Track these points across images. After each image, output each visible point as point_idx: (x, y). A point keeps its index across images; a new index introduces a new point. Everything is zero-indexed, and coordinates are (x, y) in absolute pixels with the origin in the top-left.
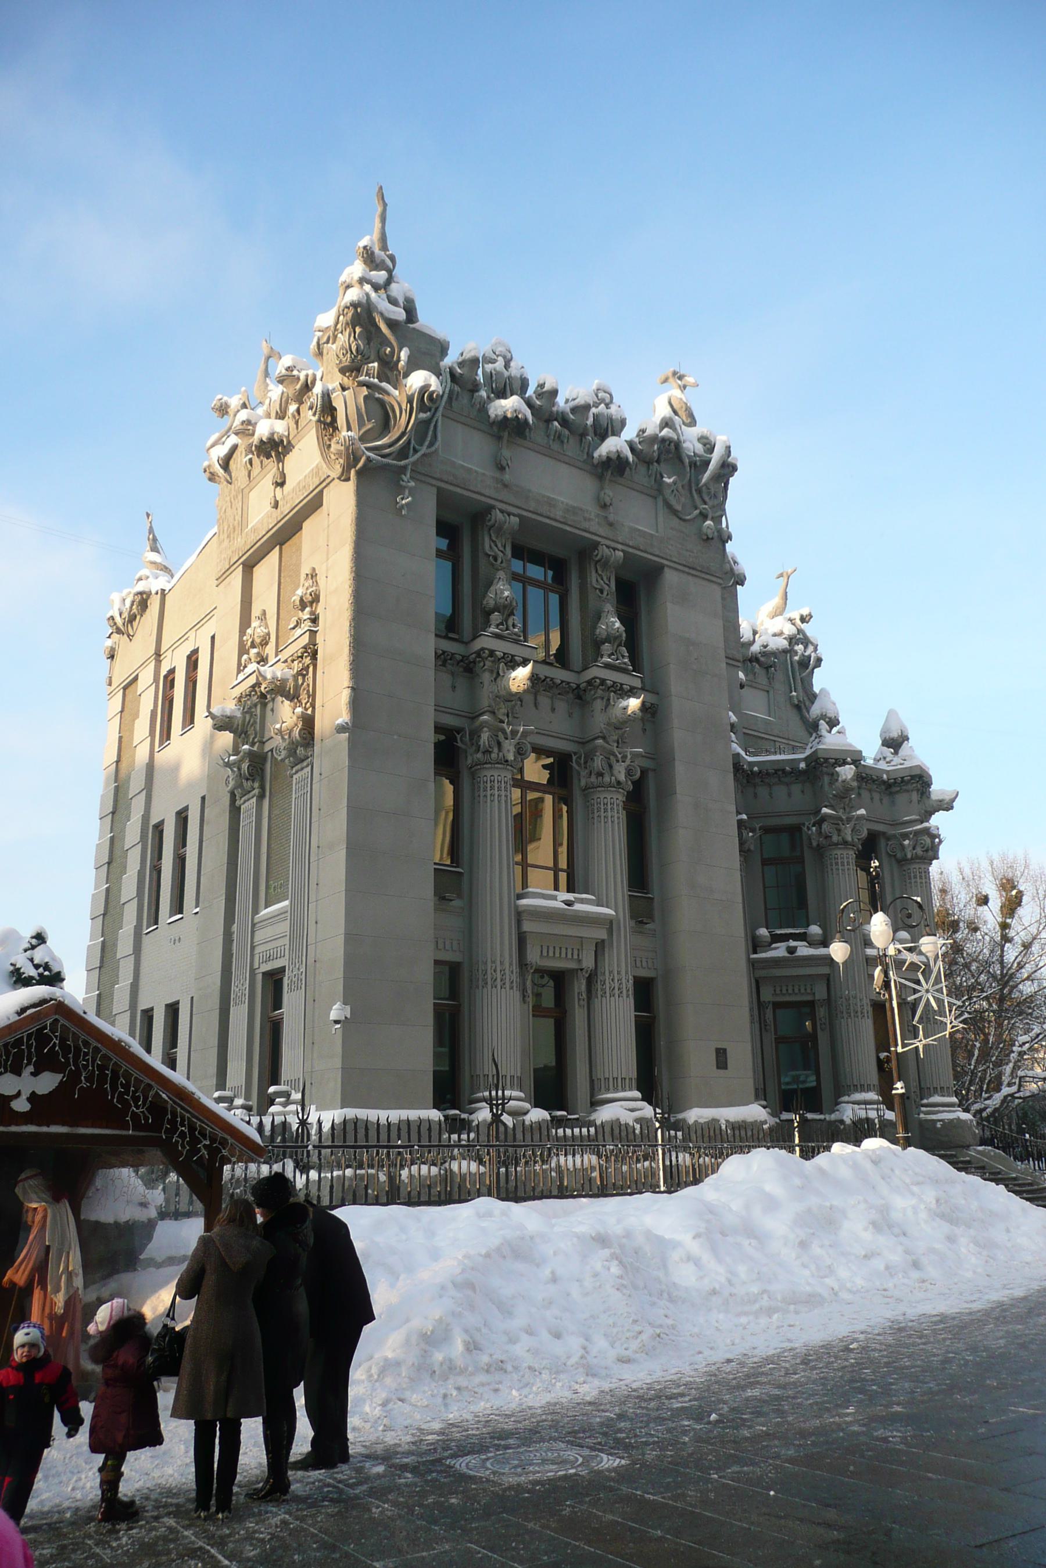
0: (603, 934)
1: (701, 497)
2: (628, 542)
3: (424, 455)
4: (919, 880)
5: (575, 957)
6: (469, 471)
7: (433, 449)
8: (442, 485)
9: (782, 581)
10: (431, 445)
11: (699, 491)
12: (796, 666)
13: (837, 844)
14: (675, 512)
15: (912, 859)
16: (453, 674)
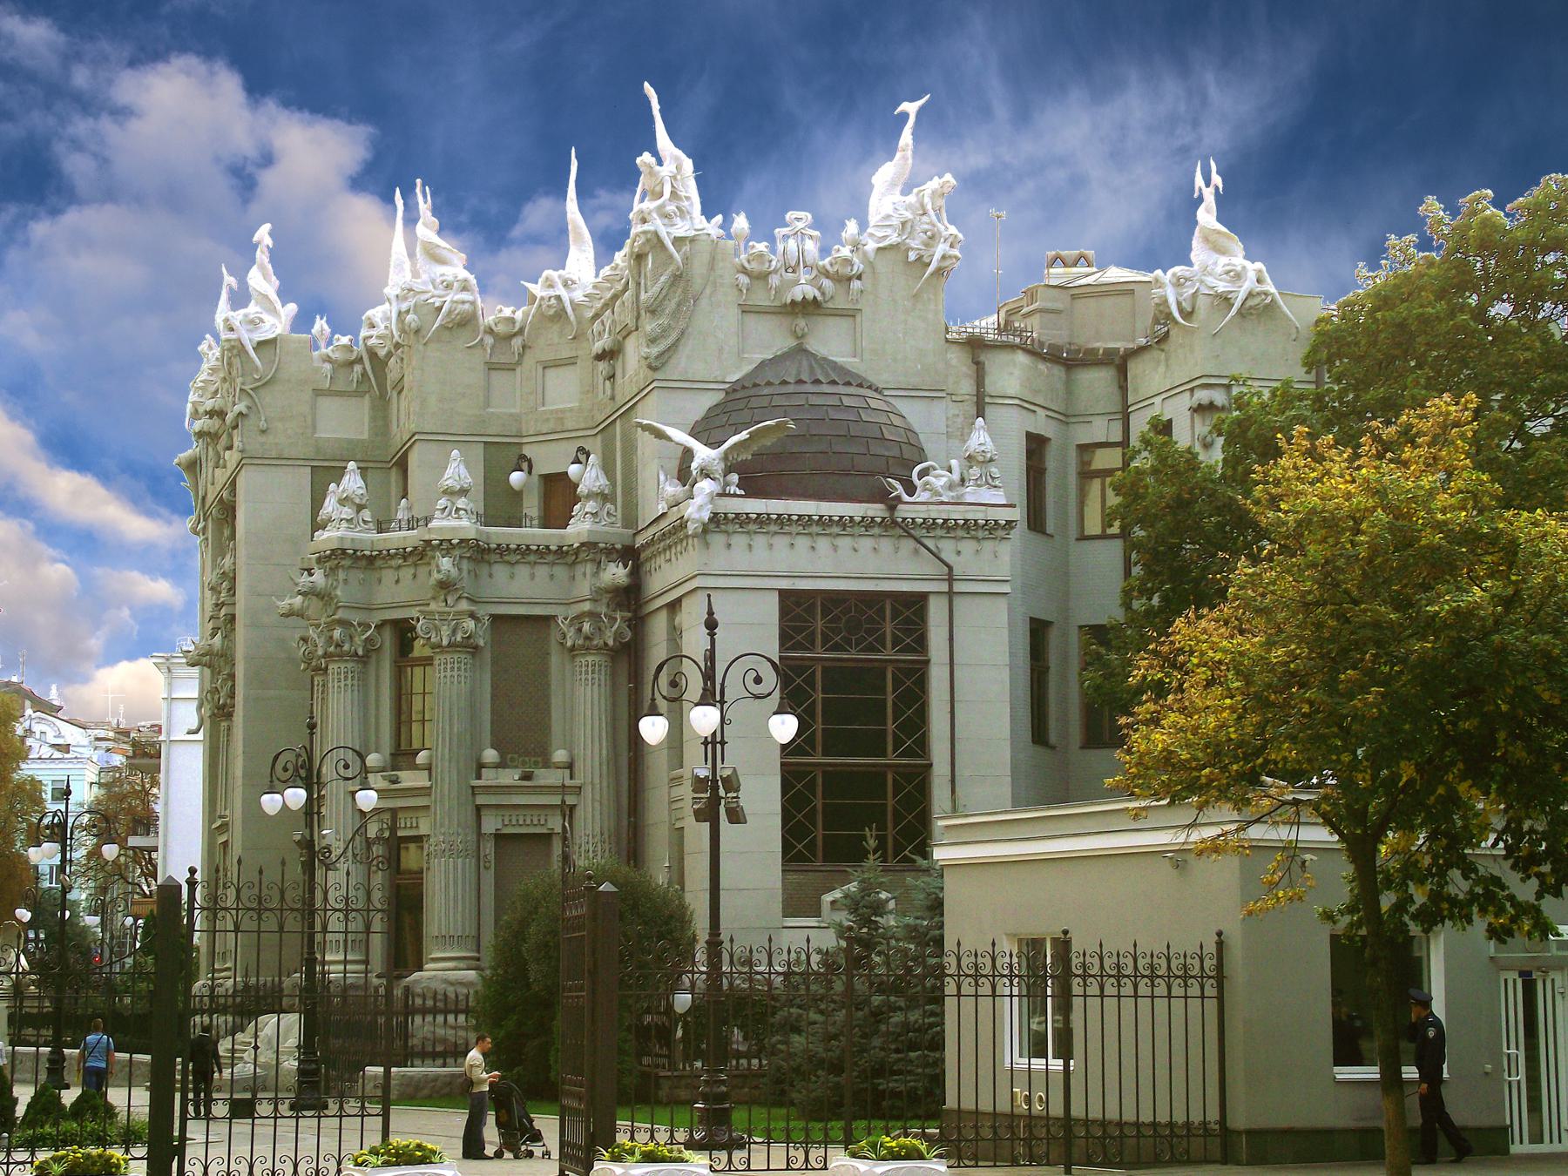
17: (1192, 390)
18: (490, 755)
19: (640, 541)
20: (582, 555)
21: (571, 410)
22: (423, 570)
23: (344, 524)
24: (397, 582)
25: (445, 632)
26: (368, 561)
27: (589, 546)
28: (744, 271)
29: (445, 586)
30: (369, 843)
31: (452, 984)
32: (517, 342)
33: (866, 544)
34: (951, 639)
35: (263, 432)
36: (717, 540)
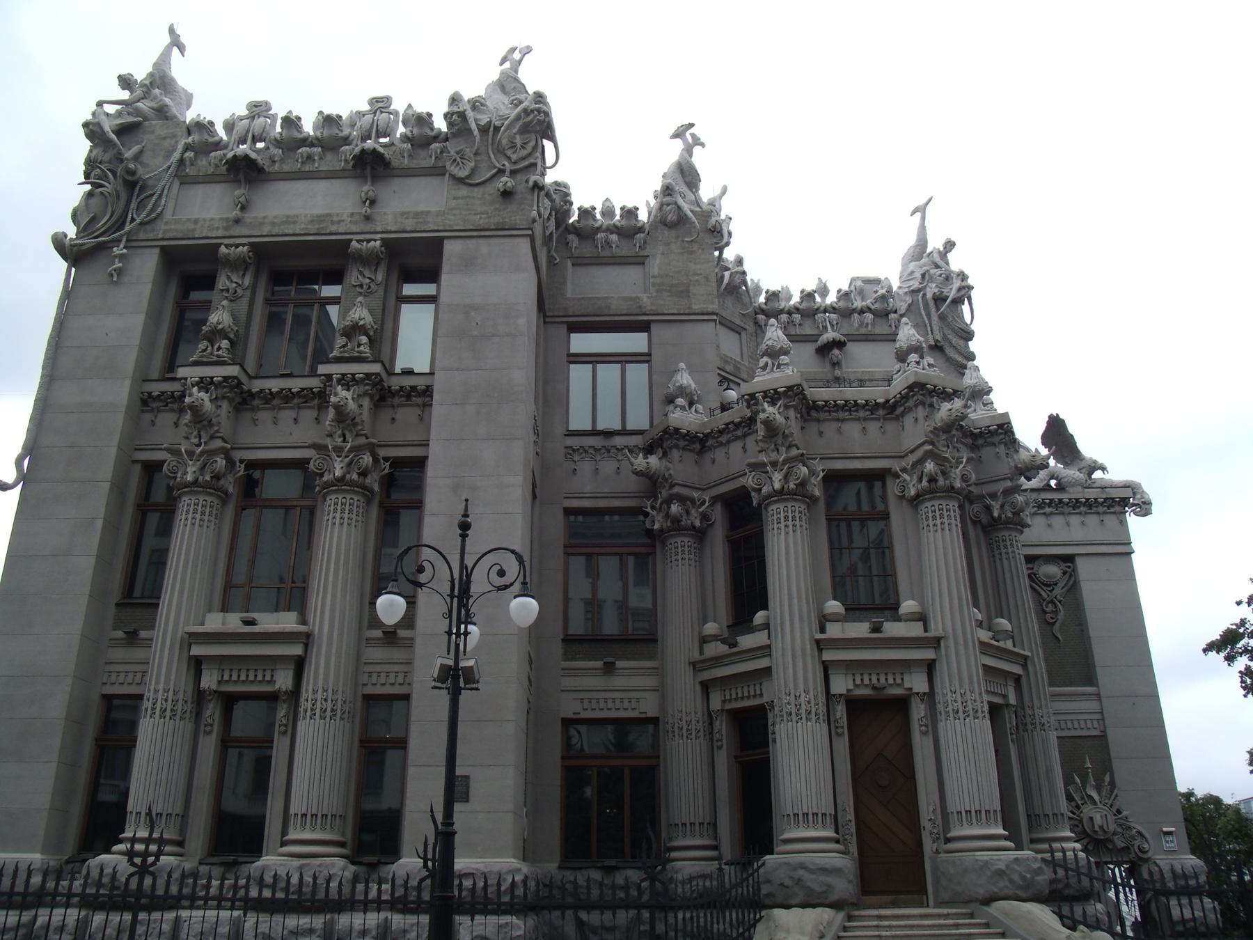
0: (297, 650)
1: (505, 155)
2: (389, 228)
3: (141, 224)
4: (931, 523)
5: (268, 678)
6: (196, 221)
7: (154, 215)
8: (165, 243)
9: (918, 215)
10: (152, 210)
11: (500, 151)
12: (931, 303)
13: (769, 496)
14: (461, 181)
15: (918, 496)
16: (172, 410)
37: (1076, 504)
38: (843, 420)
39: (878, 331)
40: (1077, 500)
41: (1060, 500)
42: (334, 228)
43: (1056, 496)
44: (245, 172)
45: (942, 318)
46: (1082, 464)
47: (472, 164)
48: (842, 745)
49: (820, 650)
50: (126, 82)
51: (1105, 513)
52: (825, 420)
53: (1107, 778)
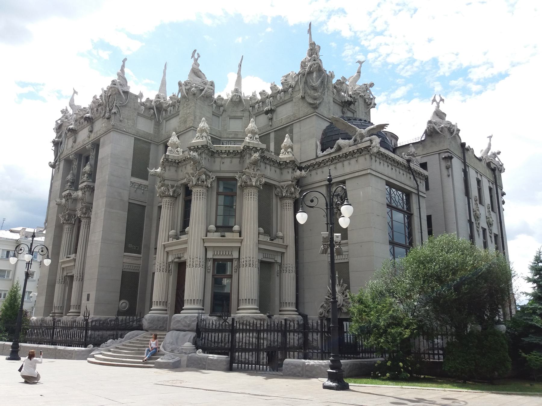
17: (439, 154)
18: (262, 230)
19: (303, 165)
20: (289, 165)
21: (241, 132)
22: (236, 161)
23: (204, 138)
24: (223, 163)
25: (254, 180)
26: (213, 154)
27: (293, 162)
28: (335, 87)
29: (255, 163)
30: (206, 259)
31: (257, 319)
32: (222, 109)
33: (401, 172)
34: (420, 208)
35: (121, 121)
36: (373, 158)
37: (346, 156)
38: (186, 164)
39: (286, 98)
40: (346, 153)
41: (339, 156)
42: (85, 143)
43: (337, 154)
44: (73, 132)
45: (306, 82)
46: (357, 133)
47: (104, 111)
48: (173, 279)
49: (165, 248)
50: (62, 112)
51: (358, 157)
52: (182, 166)
53: (342, 281)
